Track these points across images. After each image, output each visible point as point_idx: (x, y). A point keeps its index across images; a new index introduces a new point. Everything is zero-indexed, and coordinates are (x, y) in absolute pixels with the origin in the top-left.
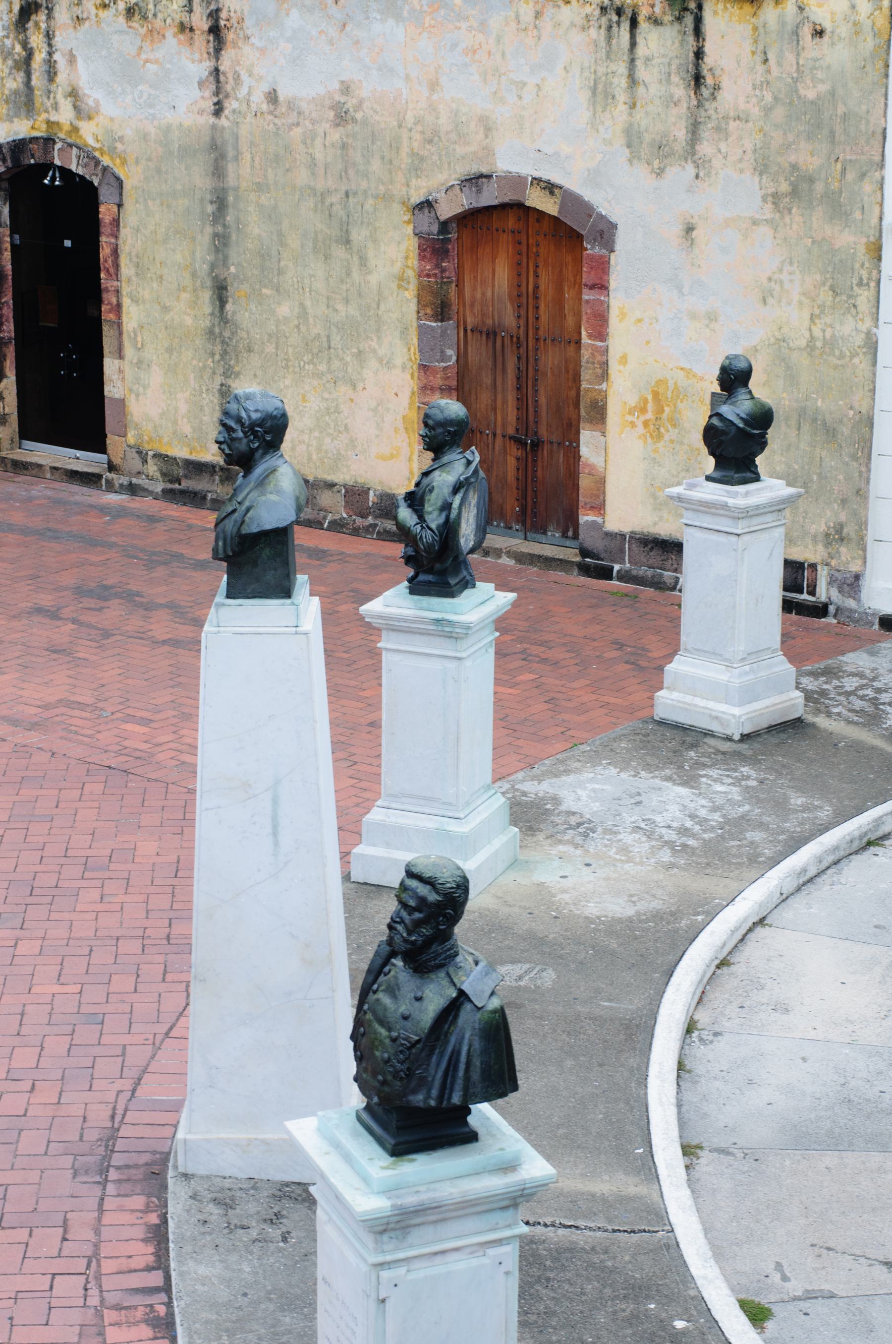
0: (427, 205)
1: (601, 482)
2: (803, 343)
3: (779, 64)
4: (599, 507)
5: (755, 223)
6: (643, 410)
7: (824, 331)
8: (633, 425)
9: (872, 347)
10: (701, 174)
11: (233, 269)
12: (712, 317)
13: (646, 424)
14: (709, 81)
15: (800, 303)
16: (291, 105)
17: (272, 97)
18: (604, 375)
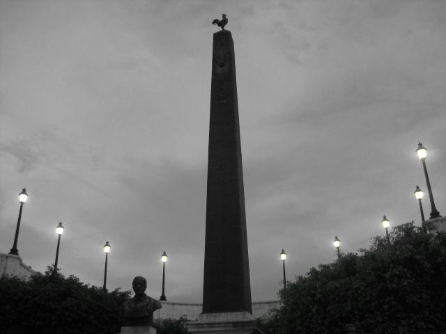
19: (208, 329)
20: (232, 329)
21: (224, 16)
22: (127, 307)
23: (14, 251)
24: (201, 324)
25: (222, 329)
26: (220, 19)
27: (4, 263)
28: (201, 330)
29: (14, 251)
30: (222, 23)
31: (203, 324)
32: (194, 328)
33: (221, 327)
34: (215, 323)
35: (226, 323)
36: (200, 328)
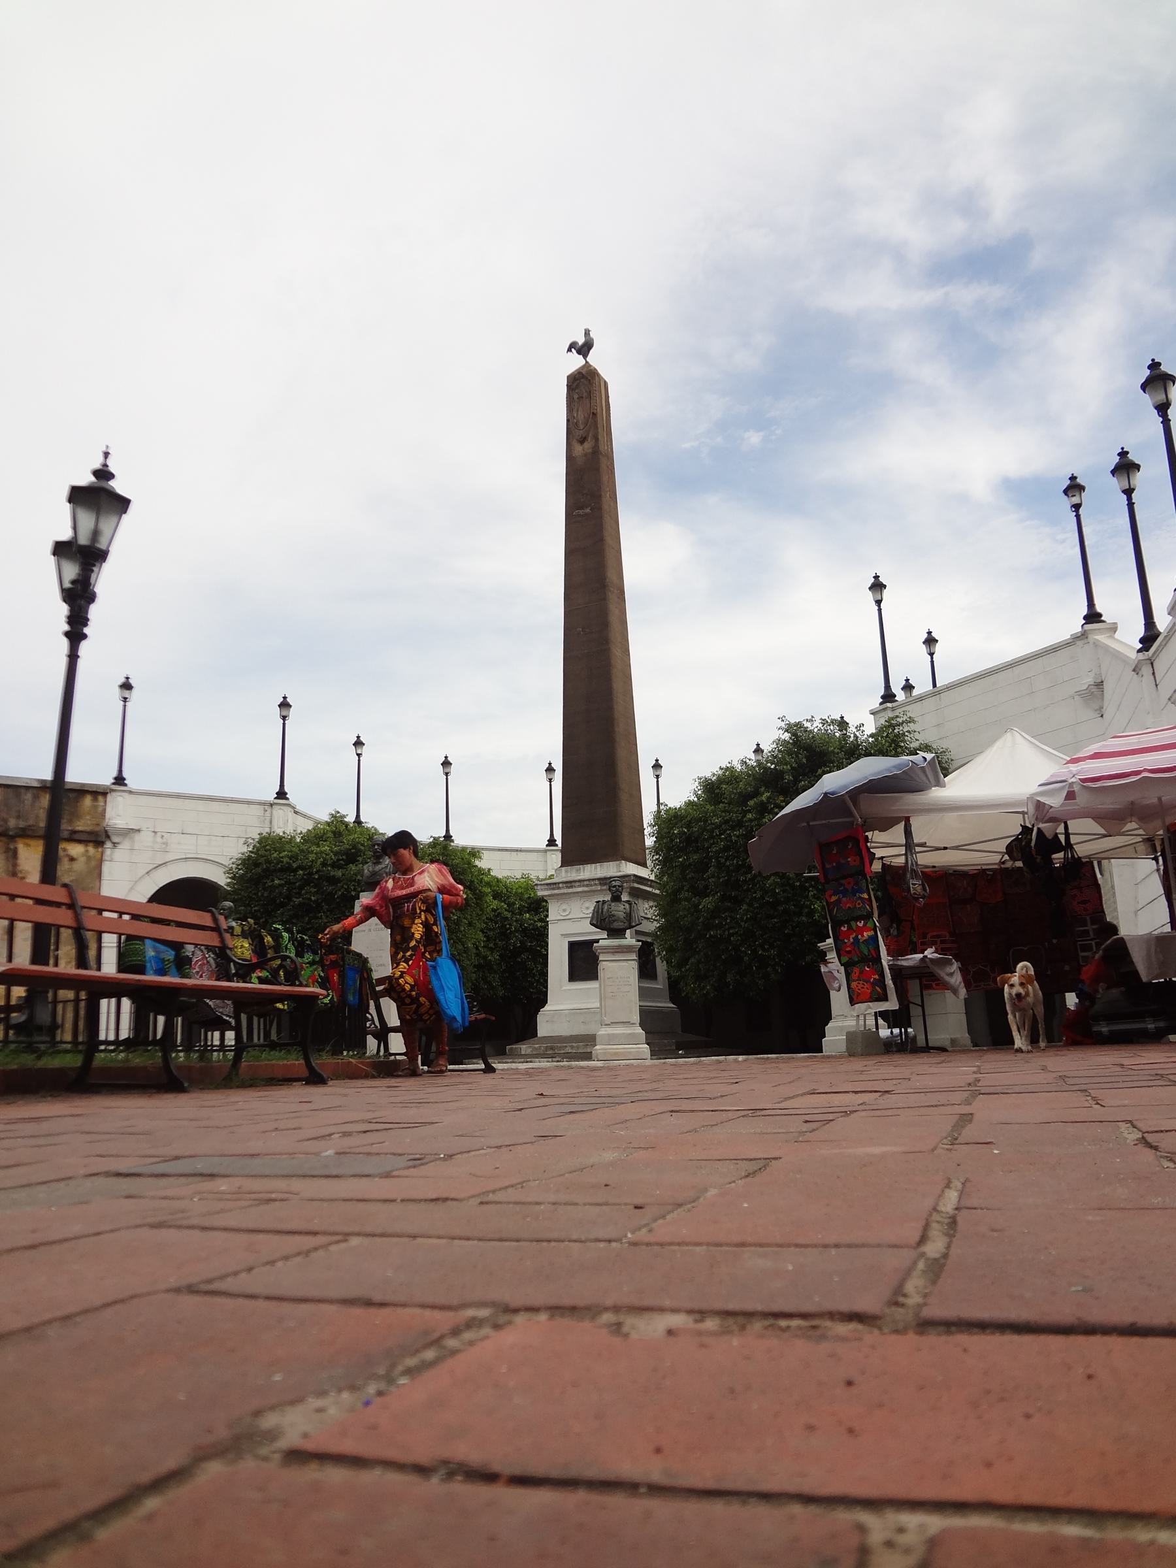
19: (566, 891)
20: (599, 888)
21: (587, 333)
22: (366, 871)
23: (282, 794)
24: (555, 884)
25: (586, 889)
26: (581, 341)
27: (268, 814)
28: (556, 892)
29: (282, 794)
30: (584, 349)
31: (559, 883)
32: (547, 889)
33: (583, 886)
34: (575, 881)
35: (589, 880)
36: (553, 889)
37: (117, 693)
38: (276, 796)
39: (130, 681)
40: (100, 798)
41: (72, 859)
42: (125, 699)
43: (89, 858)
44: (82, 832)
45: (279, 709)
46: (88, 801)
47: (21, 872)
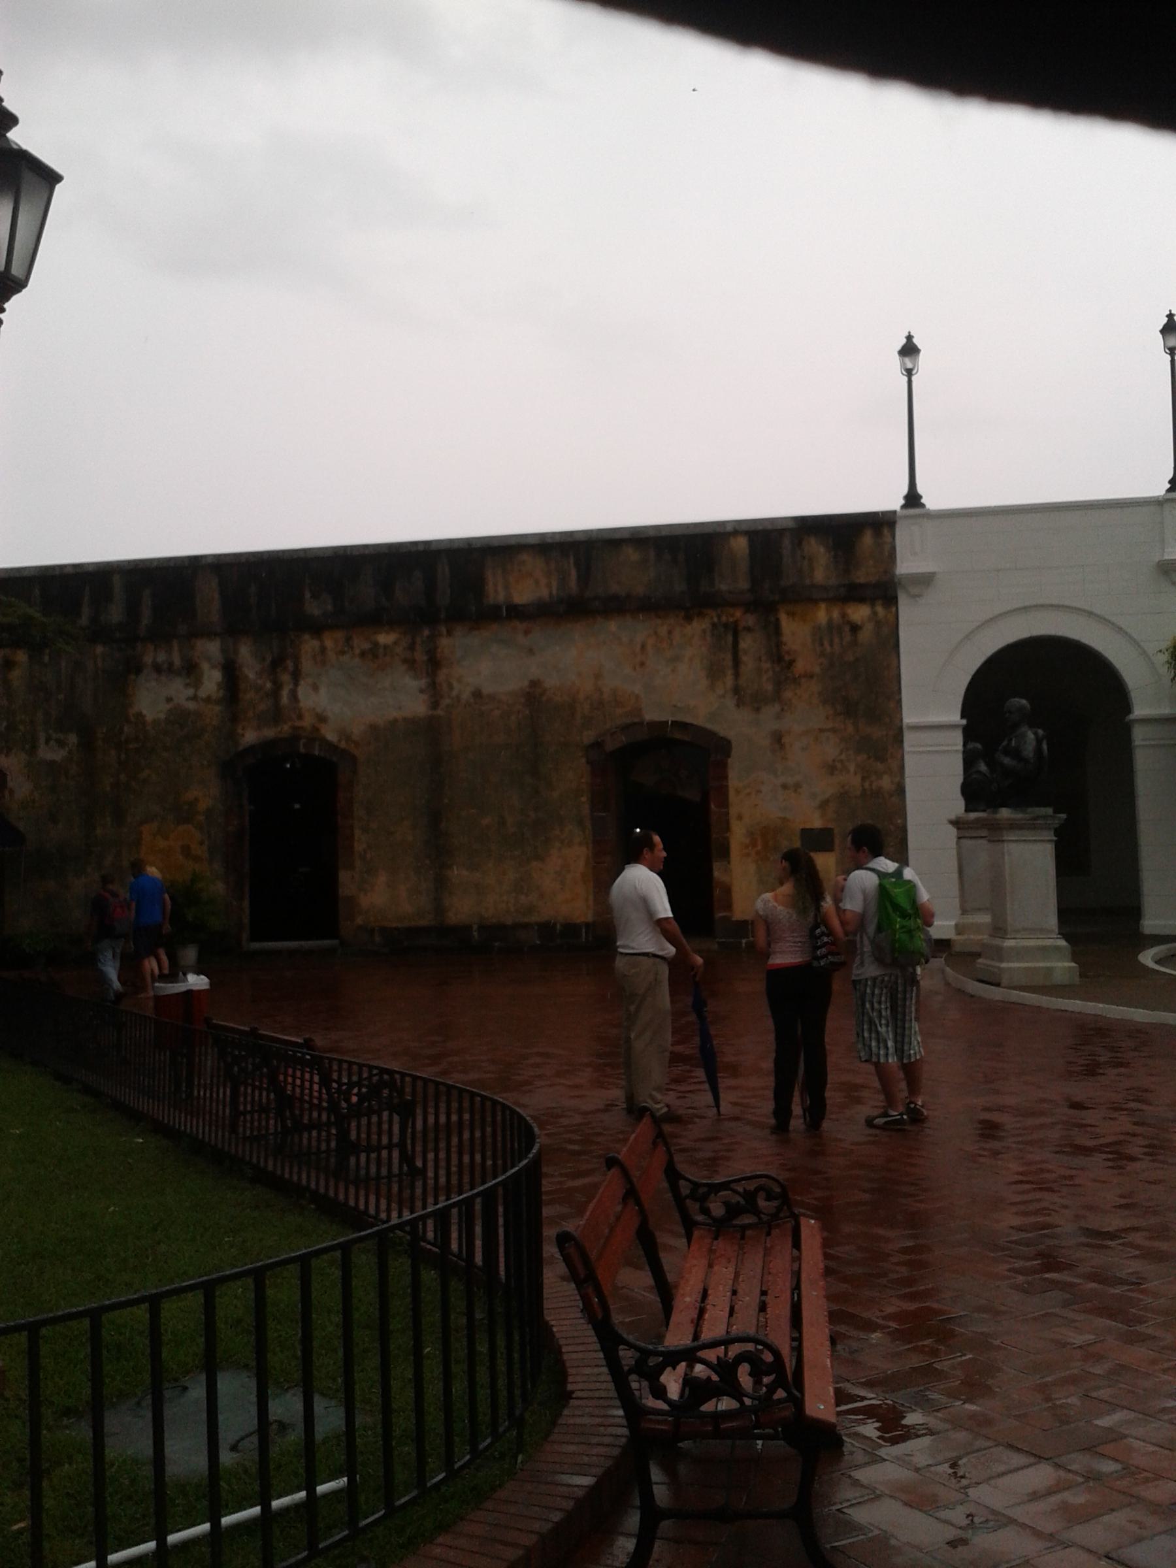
0: (597, 745)
1: (728, 890)
2: (858, 793)
3: (831, 645)
4: (729, 906)
5: (821, 730)
6: (754, 845)
7: (871, 785)
8: (748, 855)
9: (901, 790)
10: (786, 708)
11: (446, 801)
12: (797, 787)
13: (758, 853)
14: (787, 658)
15: (856, 774)
16: (492, 697)
17: (477, 694)
18: (728, 829)
37: (896, 362)
38: (1169, 486)
39: (915, 341)
40: (886, 531)
41: (855, 628)
42: (909, 373)
43: (878, 624)
44: (861, 586)
45: (1161, 336)
46: (868, 539)
47: (788, 653)
